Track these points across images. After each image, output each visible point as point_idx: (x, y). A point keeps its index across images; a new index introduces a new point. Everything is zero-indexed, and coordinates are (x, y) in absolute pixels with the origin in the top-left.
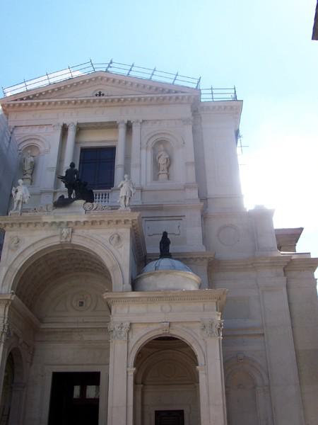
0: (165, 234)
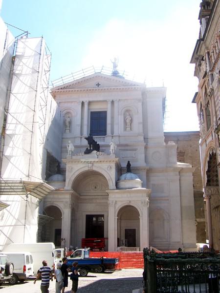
0: (129, 162)
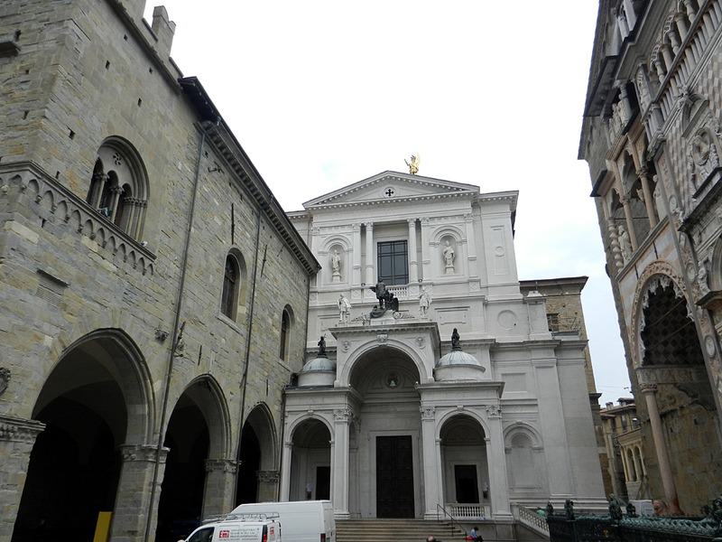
0: (455, 331)
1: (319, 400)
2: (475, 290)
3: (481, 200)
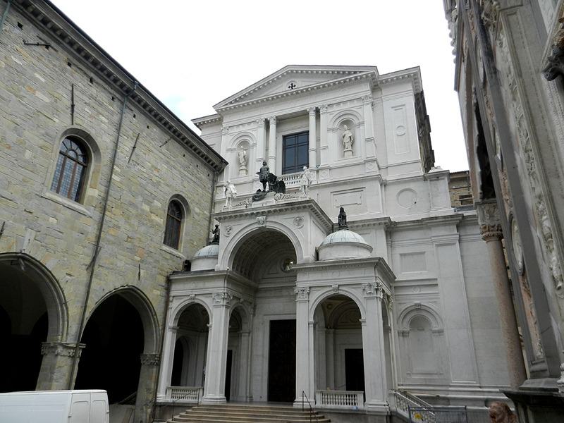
0: (342, 210)
1: (201, 285)
2: (372, 170)
3: (381, 82)
